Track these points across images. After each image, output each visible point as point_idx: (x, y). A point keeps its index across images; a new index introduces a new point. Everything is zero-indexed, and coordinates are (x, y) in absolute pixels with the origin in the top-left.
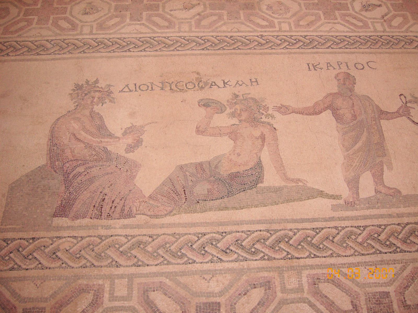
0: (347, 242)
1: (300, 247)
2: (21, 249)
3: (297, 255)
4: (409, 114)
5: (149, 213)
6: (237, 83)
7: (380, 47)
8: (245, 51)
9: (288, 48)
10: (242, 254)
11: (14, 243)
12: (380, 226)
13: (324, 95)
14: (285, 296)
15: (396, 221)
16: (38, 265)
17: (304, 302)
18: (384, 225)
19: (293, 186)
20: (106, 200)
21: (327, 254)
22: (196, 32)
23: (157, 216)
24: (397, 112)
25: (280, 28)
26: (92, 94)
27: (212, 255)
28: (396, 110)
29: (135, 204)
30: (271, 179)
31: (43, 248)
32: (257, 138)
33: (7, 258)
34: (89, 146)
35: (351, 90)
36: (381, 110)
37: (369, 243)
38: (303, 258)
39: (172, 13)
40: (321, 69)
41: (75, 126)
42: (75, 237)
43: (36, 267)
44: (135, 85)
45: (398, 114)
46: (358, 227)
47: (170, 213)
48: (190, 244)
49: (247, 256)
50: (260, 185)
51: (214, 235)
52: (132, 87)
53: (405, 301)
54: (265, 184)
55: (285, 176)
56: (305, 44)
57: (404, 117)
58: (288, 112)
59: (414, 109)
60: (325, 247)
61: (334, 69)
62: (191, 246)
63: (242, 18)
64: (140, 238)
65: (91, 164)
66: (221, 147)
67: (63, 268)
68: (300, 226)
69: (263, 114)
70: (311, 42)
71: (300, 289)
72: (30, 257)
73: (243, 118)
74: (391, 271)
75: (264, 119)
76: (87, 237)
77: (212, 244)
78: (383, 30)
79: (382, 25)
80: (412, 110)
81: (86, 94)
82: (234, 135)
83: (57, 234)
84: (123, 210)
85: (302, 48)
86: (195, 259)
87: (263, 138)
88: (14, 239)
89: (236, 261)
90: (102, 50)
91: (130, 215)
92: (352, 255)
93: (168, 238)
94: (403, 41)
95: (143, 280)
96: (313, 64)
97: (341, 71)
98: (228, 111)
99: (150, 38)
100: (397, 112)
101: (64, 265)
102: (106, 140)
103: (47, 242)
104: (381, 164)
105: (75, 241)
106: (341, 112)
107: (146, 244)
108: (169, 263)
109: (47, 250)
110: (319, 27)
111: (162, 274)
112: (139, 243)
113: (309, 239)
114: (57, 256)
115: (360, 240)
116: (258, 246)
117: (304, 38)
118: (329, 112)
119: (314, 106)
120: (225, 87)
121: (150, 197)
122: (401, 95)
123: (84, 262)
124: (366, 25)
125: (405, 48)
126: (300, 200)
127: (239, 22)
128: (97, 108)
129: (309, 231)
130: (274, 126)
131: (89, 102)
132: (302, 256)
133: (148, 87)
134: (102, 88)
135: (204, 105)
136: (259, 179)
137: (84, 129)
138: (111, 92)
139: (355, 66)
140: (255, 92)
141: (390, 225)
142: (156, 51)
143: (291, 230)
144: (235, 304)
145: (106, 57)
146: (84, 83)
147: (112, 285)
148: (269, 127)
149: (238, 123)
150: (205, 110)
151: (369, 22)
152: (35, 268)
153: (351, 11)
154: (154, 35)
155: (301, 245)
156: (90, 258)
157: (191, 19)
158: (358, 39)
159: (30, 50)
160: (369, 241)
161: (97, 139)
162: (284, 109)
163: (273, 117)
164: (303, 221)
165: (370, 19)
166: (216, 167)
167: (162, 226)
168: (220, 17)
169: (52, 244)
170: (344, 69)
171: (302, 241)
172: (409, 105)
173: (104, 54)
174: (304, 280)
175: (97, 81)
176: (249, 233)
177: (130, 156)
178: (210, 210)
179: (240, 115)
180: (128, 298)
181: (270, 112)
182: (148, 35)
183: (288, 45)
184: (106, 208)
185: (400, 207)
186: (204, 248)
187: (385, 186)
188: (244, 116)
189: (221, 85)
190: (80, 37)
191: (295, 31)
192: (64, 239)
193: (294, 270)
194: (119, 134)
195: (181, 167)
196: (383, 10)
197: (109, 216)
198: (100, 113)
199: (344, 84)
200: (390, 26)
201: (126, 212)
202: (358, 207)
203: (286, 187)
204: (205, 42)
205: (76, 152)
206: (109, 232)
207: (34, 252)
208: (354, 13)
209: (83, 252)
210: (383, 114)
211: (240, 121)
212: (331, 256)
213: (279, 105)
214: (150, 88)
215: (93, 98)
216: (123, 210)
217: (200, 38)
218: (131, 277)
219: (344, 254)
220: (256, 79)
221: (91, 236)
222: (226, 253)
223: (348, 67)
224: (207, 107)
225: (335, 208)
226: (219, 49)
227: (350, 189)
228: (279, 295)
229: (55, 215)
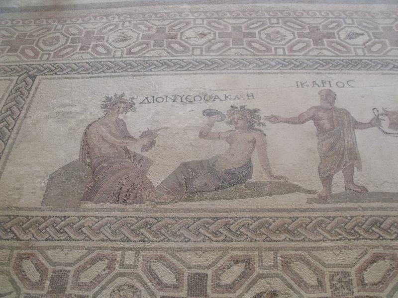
0: (318, 229)
1: (278, 232)
2: (55, 225)
3: (274, 238)
4: (380, 125)
5: (156, 200)
6: (237, 96)
7: (360, 68)
8: (245, 71)
9: (281, 69)
10: (230, 236)
11: (50, 219)
12: (347, 218)
13: (309, 107)
14: (262, 272)
15: (362, 213)
16: (67, 237)
17: (277, 277)
18: (351, 217)
19: (276, 182)
20: (123, 190)
21: (300, 239)
22: (206, 56)
23: (162, 203)
24: (369, 123)
25: (276, 53)
26: (119, 104)
27: (205, 236)
28: (369, 122)
29: (146, 192)
30: (258, 175)
31: (72, 224)
32: (249, 142)
33: (44, 231)
34: (113, 146)
35: (332, 103)
36: (356, 122)
37: (336, 231)
38: (280, 241)
39: (188, 40)
40: (308, 86)
41: (104, 129)
42: (96, 217)
43: (65, 239)
44: (153, 97)
45: (370, 125)
46: (328, 218)
47: (172, 201)
48: (187, 226)
49: (233, 238)
50: (249, 180)
51: (207, 219)
52: (150, 99)
53: (364, 281)
54: (254, 179)
55: (270, 174)
56: (296, 66)
58: (277, 121)
59: (384, 120)
60: (299, 233)
61: (319, 86)
62: (188, 227)
63: (245, 45)
64: (147, 220)
65: (113, 160)
66: (219, 148)
67: (86, 240)
68: (278, 215)
69: (255, 122)
70: (301, 64)
71: (275, 266)
72: (62, 231)
73: (238, 125)
74: (353, 254)
75: (256, 127)
76: (106, 217)
77: (205, 227)
78: (363, 54)
79: (363, 49)
80: (382, 122)
81: (114, 105)
82: (230, 140)
83: (83, 214)
84: (135, 197)
85: (293, 69)
86: (190, 238)
87: (254, 142)
88: (50, 217)
89: (224, 241)
90: (129, 70)
91: (141, 201)
92: (321, 241)
93: (169, 221)
94: (380, 64)
95: (147, 253)
96: (301, 82)
97: (323, 88)
98: (227, 119)
99: (168, 60)
100: (370, 123)
101: (87, 238)
102: (127, 141)
103: (75, 220)
104: (353, 166)
105: (97, 220)
106: (322, 122)
107: (152, 225)
108: (169, 240)
109: (74, 226)
110: (309, 52)
111: (162, 249)
112: (147, 223)
113: (286, 226)
114: (82, 231)
115: (328, 228)
116: (242, 230)
117: (296, 61)
119: (299, 117)
120: (226, 100)
121: (158, 187)
122: (374, 109)
123: (102, 236)
124: (349, 51)
125: (381, 70)
126: (281, 193)
127: (243, 48)
128: (121, 116)
129: (286, 219)
130: (264, 133)
131: (116, 110)
132: (278, 239)
133: (163, 99)
134: (126, 100)
135: (208, 115)
136: (249, 176)
137: (110, 132)
138: (134, 104)
139: (337, 85)
140: (251, 105)
141: (356, 216)
142: (173, 70)
143: (271, 218)
144: (220, 275)
145: (132, 75)
146: (113, 96)
147: (123, 255)
148: (260, 133)
149: (234, 129)
150: (209, 118)
151: (352, 48)
152: (65, 240)
153: (337, 39)
154: (172, 58)
155: (279, 231)
156: (107, 234)
157: (203, 45)
158: (341, 62)
159: (73, 70)
160: (336, 229)
161: (120, 140)
162: (274, 119)
163: (264, 125)
164: (281, 210)
165: (353, 45)
166: (213, 165)
167: (166, 211)
168: (227, 44)
169: (79, 222)
170: (327, 87)
171: (280, 227)
172: (380, 117)
173: (131, 73)
174: (279, 258)
175: (123, 95)
176: (236, 219)
177: (145, 154)
178: (206, 199)
179: (236, 123)
180: (135, 266)
181: (262, 121)
182: (168, 58)
183: (281, 67)
184: (123, 195)
186: (198, 230)
187: (354, 185)
188: (241, 123)
189: (223, 98)
190: (113, 60)
191: (289, 56)
192: (89, 218)
193: (271, 251)
194: (137, 137)
195: (185, 165)
196: (366, 38)
197: (124, 201)
198: (124, 119)
199: (326, 99)
200: (370, 51)
201: (138, 198)
203: (270, 183)
204: (213, 64)
205: (102, 150)
206: (124, 214)
207: (65, 227)
208: (339, 41)
209: (102, 229)
210: (358, 125)
211: (236, 128)
212: (303, 240)
213: (270, 115)
214: (165, 100)
215: (119, 107)
216: (135, 197)
217: (209, 61)
218: (137, 251)
219: (314, 239)
220: (252, 94)
221: (109, 217)
222: (216, 234)
223: (330, 84)
224: (210, 116)
225: (309, 201)
226: (224, 69)
227: (324, 186)
228: (257, 269)
229: (82, 200)
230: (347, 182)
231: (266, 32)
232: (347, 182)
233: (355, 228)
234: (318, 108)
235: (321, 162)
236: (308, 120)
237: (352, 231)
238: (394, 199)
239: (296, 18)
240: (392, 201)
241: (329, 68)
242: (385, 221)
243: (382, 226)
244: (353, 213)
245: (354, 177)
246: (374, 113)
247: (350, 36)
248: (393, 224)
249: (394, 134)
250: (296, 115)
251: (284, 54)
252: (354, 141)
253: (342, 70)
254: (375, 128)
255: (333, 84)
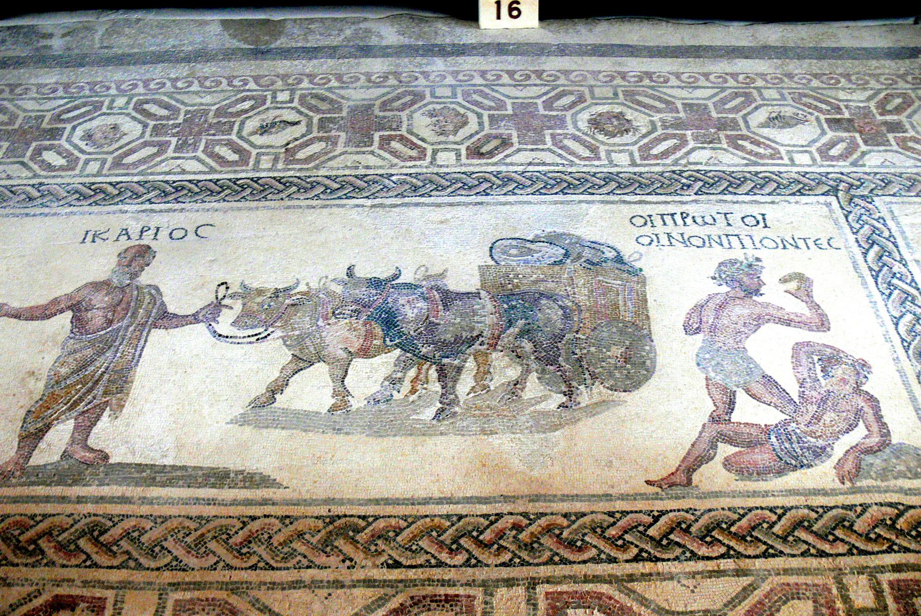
4: (214, 320)
24: (193, 315)
45: (195, 319)
57: (201, 324)
61: (129, 238)
80: (224, 310)
118: (69, 314)
141: (54, 515)
158: (212, 186)
170: (147, 240)
172: (224, 302)
185: (90, 485)
202: (14, 481)
223: (156, 234)
230: (73, 441)
231: (87, 126)
232: (73, 442)
233: (40, 542)
234: (96, 286)
235: (41, 399)
236: (62, 311)
237: (32, 547)
238: (158, 479)
239: (170, 95)
240: (152, 482)
241: (175, 199)
242: (114, 526)
243: (102, 539)
244: (49, 508)
245: (93, 431)
246: (217, 292)
247: (264, 130)
248: (129, 533)
249: (236, 337)
250: (43, 301)
251: (99, 174)
252: (137, 353)
253: (204, 202)
254: (202, 327)
255: (164, 234)
